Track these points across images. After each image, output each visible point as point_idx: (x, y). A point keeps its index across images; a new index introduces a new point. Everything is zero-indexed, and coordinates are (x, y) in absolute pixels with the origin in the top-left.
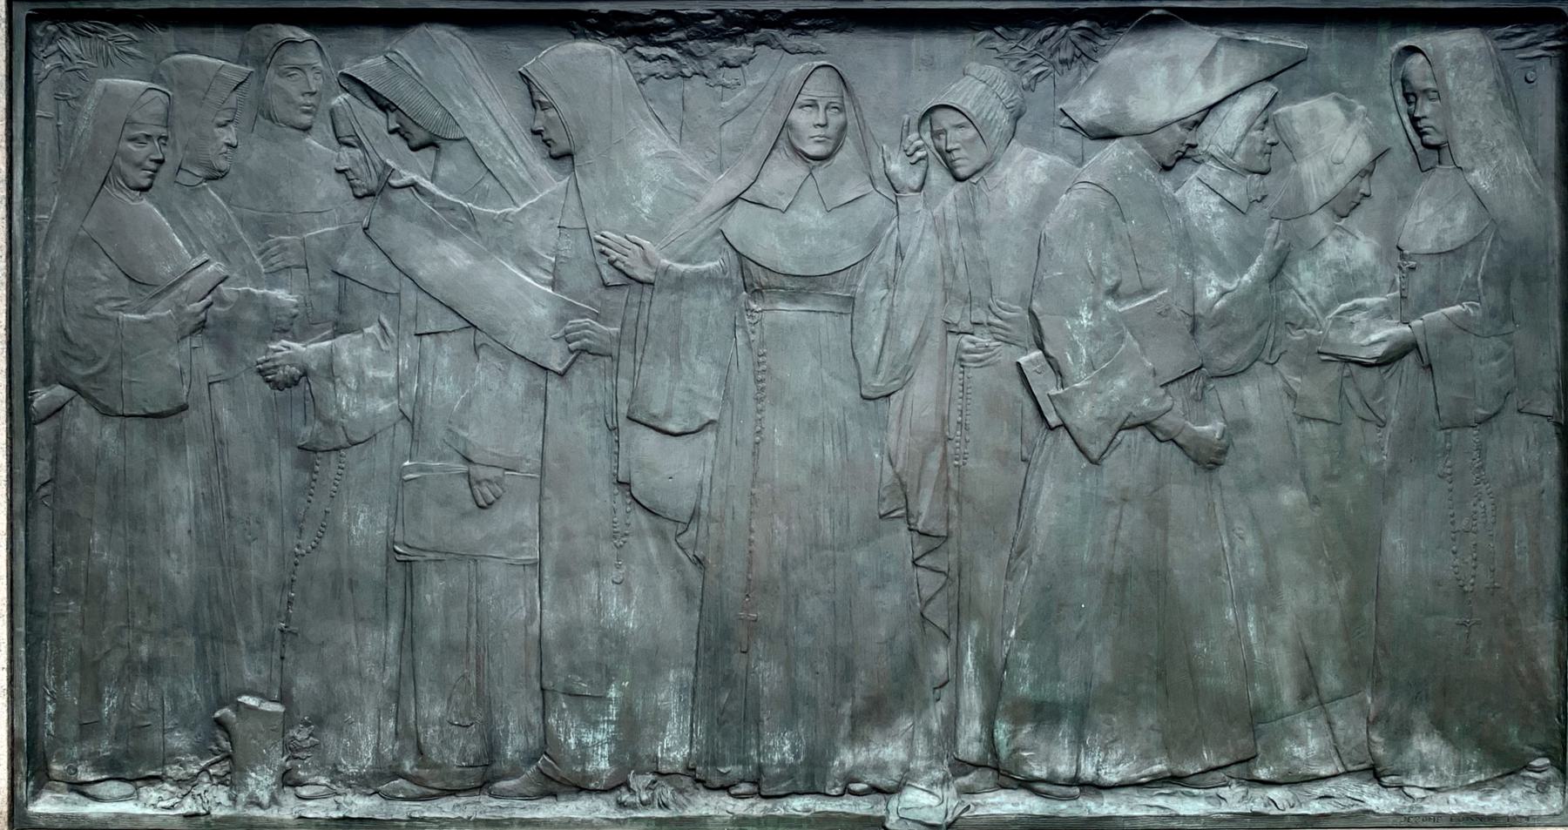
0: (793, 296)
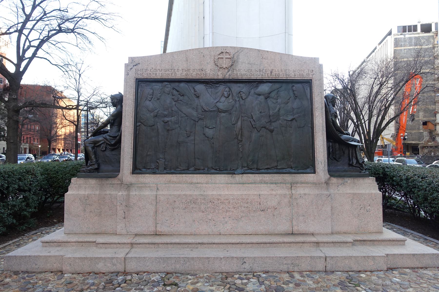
0: (224, 113)
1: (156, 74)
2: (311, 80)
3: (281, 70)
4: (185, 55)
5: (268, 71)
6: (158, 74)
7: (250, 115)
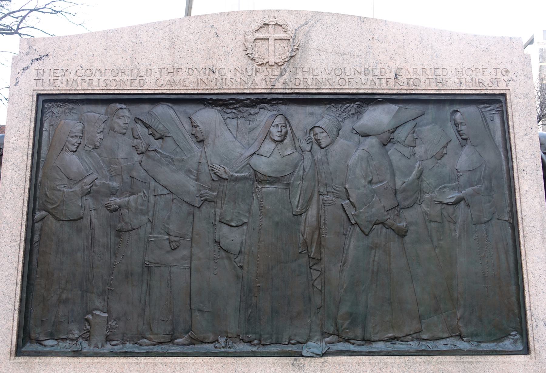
0: (271, 183)
1: (91, 83)
2: (504, 95)
3: (424, 70)
4: (167, 34)
5: (388, 71)
6: (96, 83)
7: (341, 188)
